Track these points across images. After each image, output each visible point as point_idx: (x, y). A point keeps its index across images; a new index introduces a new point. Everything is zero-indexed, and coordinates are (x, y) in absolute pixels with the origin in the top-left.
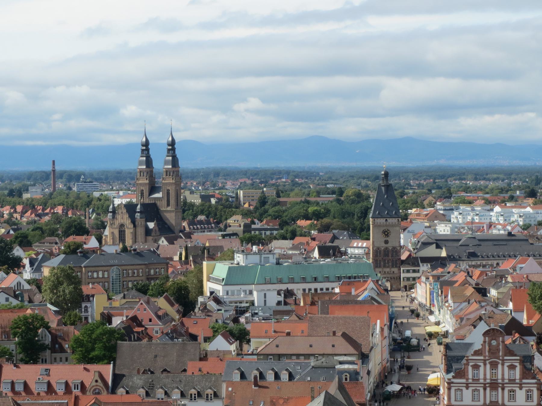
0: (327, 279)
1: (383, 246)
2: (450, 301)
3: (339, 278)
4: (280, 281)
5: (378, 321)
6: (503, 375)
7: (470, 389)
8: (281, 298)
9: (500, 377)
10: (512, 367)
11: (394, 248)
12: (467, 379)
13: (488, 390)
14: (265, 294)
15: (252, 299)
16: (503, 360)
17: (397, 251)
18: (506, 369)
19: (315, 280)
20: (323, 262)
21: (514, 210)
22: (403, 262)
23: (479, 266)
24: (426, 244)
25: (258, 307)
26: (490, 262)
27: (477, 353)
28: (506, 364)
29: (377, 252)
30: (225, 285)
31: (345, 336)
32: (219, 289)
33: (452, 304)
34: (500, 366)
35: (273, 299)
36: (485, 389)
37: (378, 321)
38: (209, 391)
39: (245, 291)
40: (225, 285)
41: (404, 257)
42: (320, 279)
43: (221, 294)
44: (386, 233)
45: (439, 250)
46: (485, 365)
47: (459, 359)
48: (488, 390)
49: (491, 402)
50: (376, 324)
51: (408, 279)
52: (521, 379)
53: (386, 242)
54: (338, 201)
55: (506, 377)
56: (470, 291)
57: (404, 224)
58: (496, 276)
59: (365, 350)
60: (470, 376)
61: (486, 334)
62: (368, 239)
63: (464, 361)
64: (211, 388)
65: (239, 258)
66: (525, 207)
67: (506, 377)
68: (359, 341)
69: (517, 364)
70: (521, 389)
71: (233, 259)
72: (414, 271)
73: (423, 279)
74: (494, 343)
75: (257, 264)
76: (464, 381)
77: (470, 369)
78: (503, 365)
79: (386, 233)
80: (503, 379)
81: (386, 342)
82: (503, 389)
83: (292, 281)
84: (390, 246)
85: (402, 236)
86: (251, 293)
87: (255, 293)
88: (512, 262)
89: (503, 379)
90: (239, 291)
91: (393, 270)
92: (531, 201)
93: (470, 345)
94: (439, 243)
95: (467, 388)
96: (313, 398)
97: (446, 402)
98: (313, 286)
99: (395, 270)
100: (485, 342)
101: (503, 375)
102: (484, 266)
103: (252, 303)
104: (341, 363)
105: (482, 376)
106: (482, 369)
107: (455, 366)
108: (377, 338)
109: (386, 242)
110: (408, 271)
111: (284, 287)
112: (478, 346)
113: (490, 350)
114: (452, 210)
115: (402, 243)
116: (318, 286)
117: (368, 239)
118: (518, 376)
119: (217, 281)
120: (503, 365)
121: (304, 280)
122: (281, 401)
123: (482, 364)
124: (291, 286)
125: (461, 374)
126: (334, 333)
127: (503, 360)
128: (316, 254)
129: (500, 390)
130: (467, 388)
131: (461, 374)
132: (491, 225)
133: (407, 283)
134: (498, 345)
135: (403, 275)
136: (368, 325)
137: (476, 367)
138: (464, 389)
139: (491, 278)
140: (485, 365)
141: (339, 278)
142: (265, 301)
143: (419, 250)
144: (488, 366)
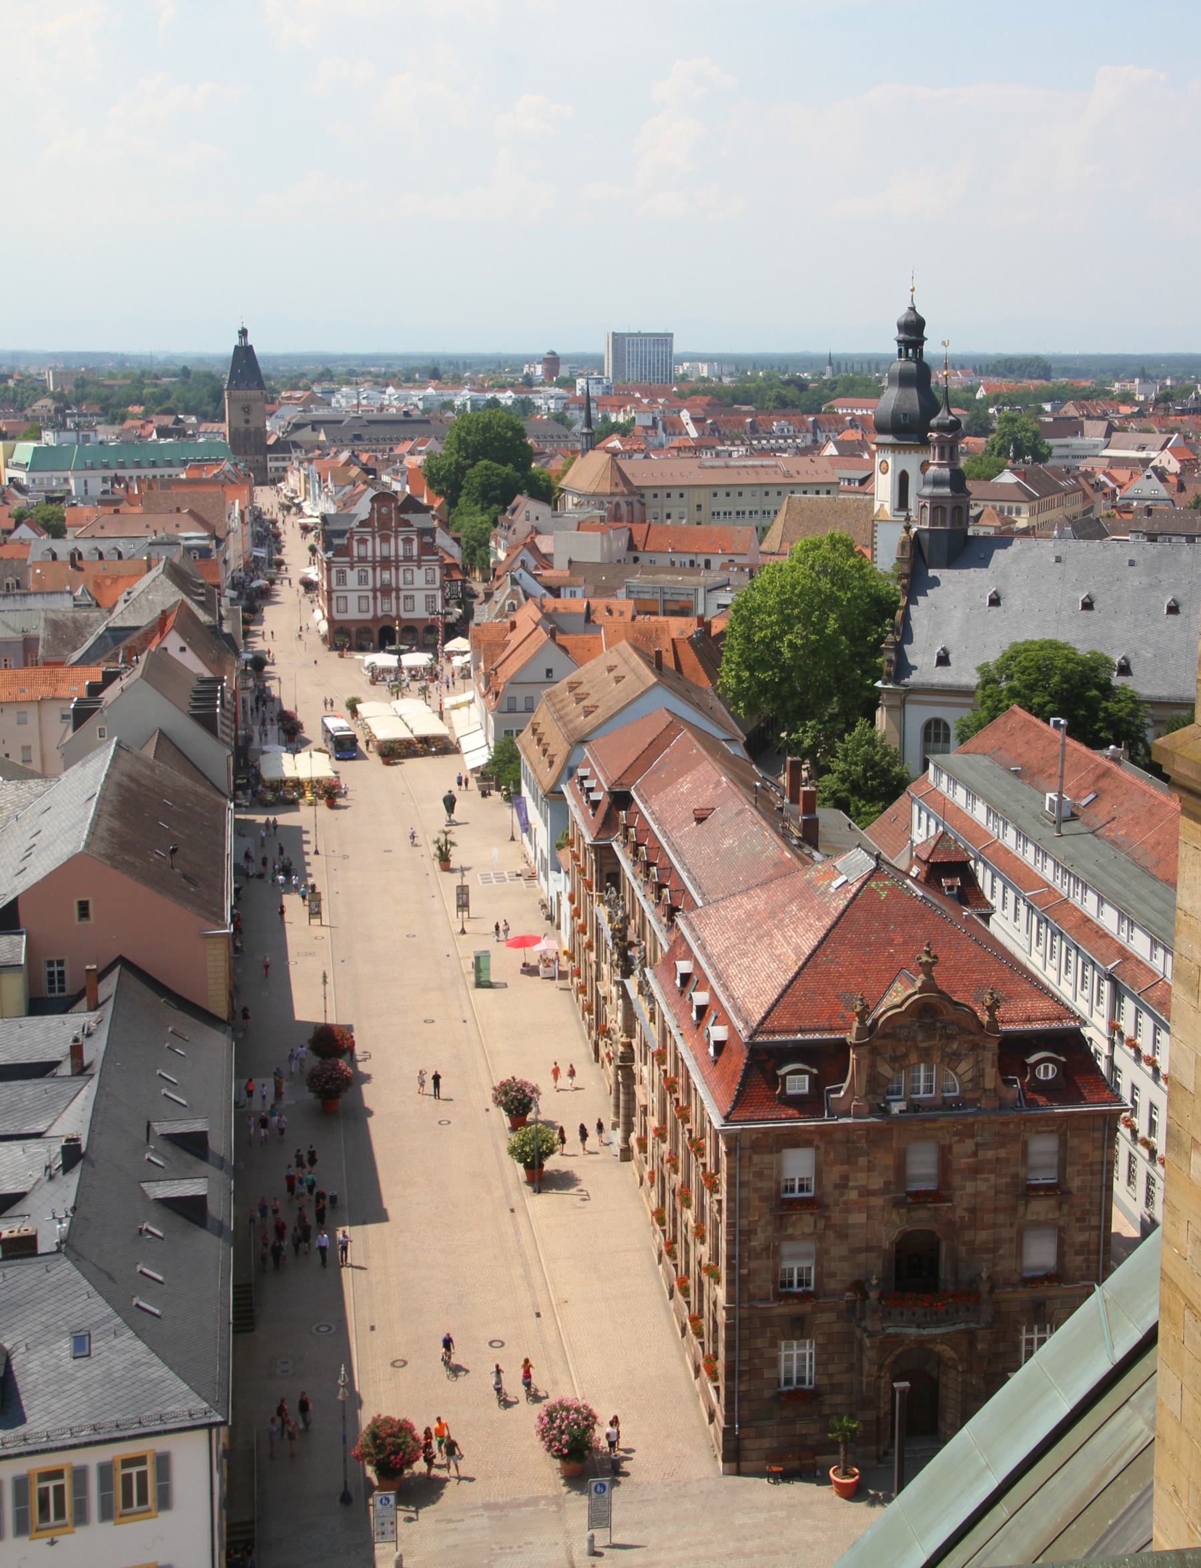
0: (170, 464)
1: (242, 426)
2: (330, 486)
3: (185, 463)
4: (106, 466)
5: (237, 502)
6: (397, 550)
7: (356, 570)
8: (108, 486)
9: (393, 553)
10: (408, 541)
11: (258, 429)
12: (352, 557)
13: (378, 570)
14: (86, 482)
15: (68, 488)
16: (396, 532)
17: (262, 434)
18: (401, 544)
19: (154, 465)
20: (162, 441)
21: (412, 393)
22: (270, 449)
23: (367, 451)
24: (298, 426)
25: (76, 497)
26: (381, 447)
27: (363, 524)
28: (401, 537)
29: (234, 433)
30: (30, 471)
31: (191, 513)
32: (21, 476)
33: (333, 489)
34: (393, 541)
35: (97, 487)
36: (374, 569)
37: (237, 502)
38: (11, 580)
39: (58, 479)
40: (30, 471)
41: (271, 442)
42: (160, 463)
43: (25, 483)
44: (247, 410)
45: (315, 433)
46: (374, 539)
47: (341, 534)
48: (378, 570)
49: (382, 585)
50: (234, 504)
51: (277, 469)
52: (419, 555)
53: (247, 421)
54: (184, 383)
55: (401, 552)
56: (355, 471)
57: (269, 408)
58: (388, 460)
59: (220, 534)
60: (355, 554)
61: (373, 500)
62: (223, 420)
63: (348, 535)
64: (11, 575)
65: (49, 438)
66: (426, 388)
67: (401, 552)
68: (214, 522)
69: (414, 537)
70: (419, 567)
71: (40, 438)
72: (284, 459)
73: (296, 464)
74: (384, 510)
75: (74, 444)
76: (347, 559)
77: (355, 544)
78: (396, 538)
79: (247, 410)
80: (397, 555)
81: (248, 530)
82: (397, 569)
83: (122, 466)
84: (252, 426)
85: (268, 423)
86: (66, 480)
87: (72, 482)
88: (409, 445)
89: (397, 555)
90: (50, 479)
91: (257, 457)
92: (434, 383)
93: (355, 515)
94: (316, 425)
95: (352, 568)
96: (149, 569)
97: (325, 587)
98: (150, 472)
99: (260, 458)
100: (373, 509)
101: (397, 550)
102: (374, 451)
103: (69, 491)
104: (187, 539)
105: (370, 553)
106: (370, 544)
107: (337, 541)
108: (235, 523)
109: (247, 421)
110: (276, 459)
111: (110, 473)
112: (365, 515)
113: (379, 519)
114: (332, 392)
115: (268, 429)
116: (158, 472)
117: (223, 420)
118: (415, 552)
119: (18, 466)
120: (396, 538)
121: (138, 465)
122: (108, 582)
123: (370, 538)
124: (121, 473)
125: (344, 551)
126: (178, 510)
127: (396, 532)
128: (155, 436)
129: (393, 569)
130: (352, 568)
131: (344, 551)
132: (381, 409)
133: (276, 475)
134: (390, 512)
135: (270, 464)
136: (222, 506)
137: (363, 541)
138: (348, 570)
139: (384, 460)
140: (374, 539)
141: (185, 463)
142: (86, 491)
143: (290, 433)
144: (378, 540)
